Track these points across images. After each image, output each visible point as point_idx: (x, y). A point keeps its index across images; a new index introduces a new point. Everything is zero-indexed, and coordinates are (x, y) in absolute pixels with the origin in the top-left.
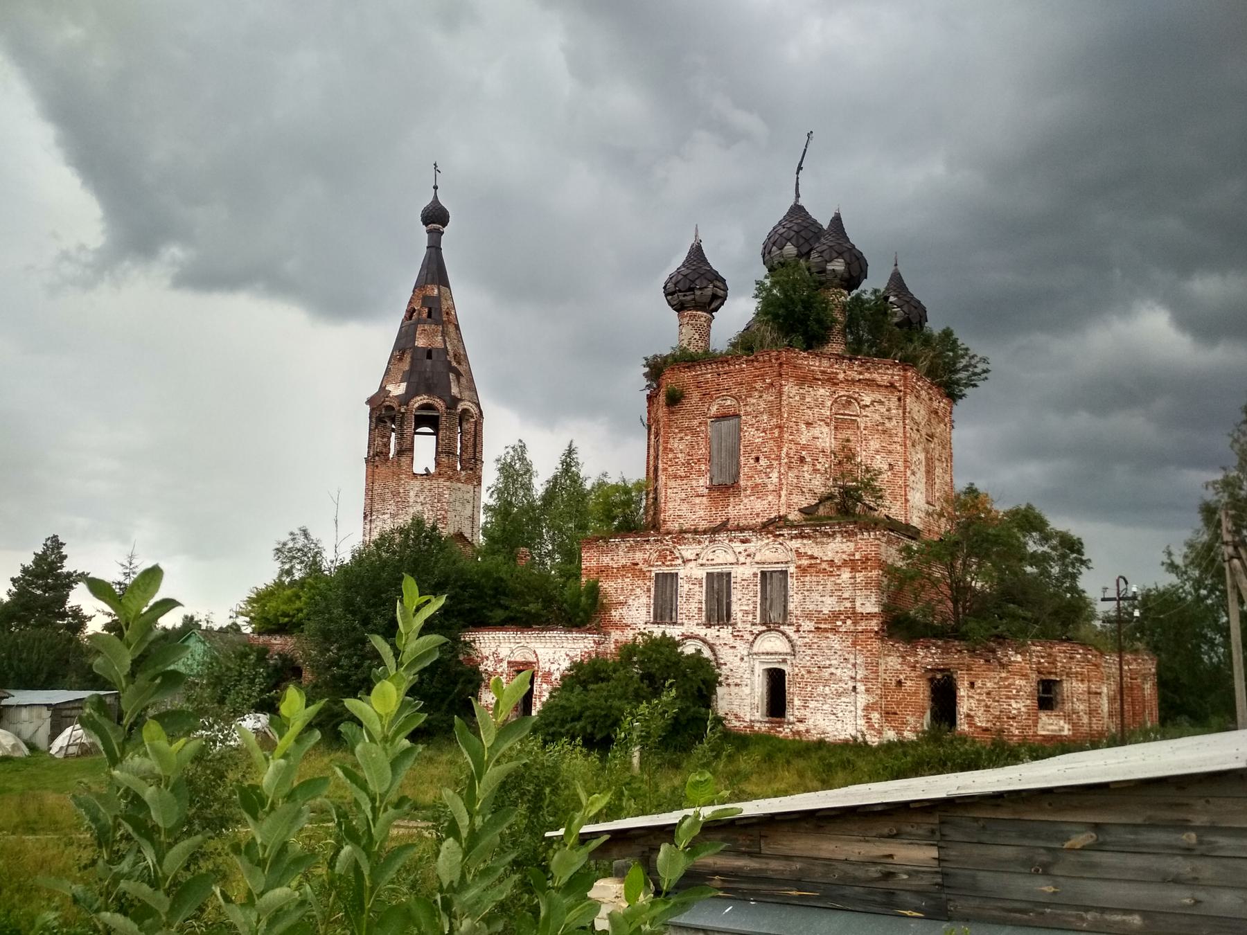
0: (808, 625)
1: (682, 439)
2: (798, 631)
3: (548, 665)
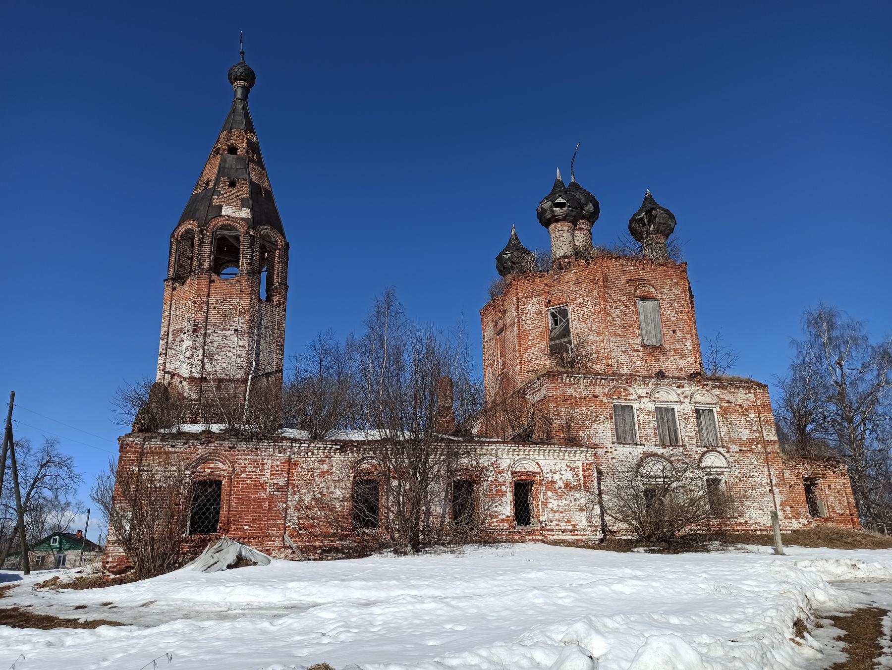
0: (735, 448)
1: (616, 308)
2: (728, 452)
3: (550, 475)
